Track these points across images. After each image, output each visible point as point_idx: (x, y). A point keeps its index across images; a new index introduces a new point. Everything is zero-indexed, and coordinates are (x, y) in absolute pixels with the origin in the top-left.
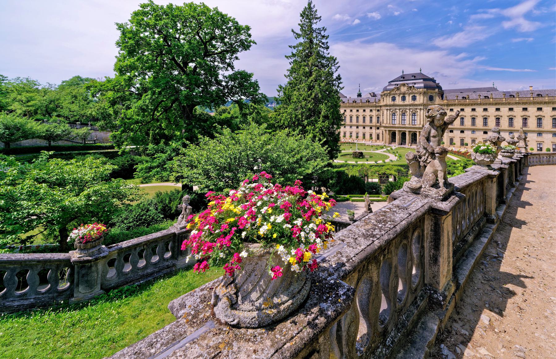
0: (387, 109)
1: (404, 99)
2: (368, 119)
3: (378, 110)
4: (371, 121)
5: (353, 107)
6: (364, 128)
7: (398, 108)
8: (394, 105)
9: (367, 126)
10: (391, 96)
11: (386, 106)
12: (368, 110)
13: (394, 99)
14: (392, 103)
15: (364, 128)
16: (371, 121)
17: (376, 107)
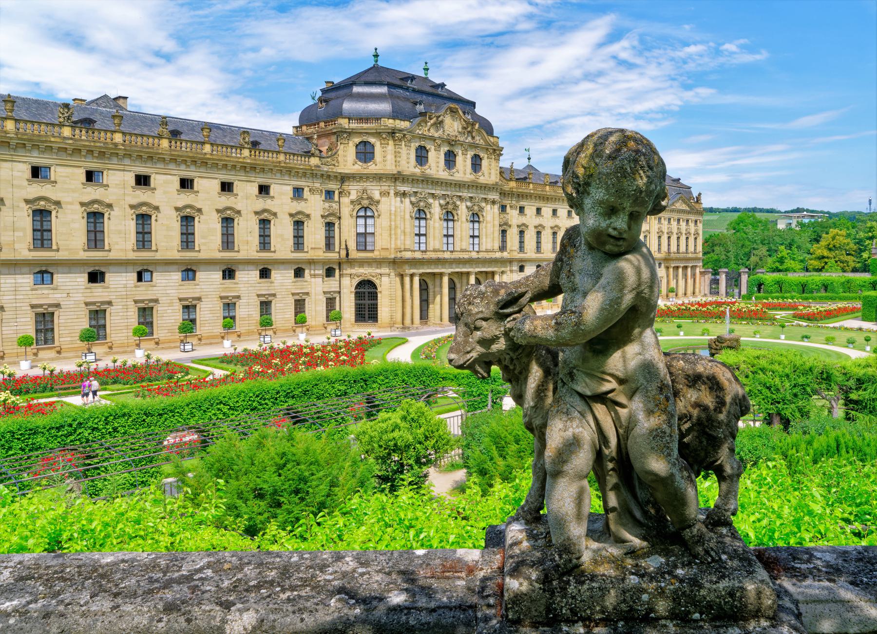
0: (404, 194)
1: (450, 159)
2: (282, 233)
3: (329, 194)
4: (299, 241)
5: (203, 163)
6: (265, 273)
7: (438, 192)
8: (427, 180)
9: (283, 263)
10: (415, 145)
11: (397, 178)
12: (282, 190)
13: (422, 156)
14: (418, 171)
15: (265, 273)
16: (299, 241)
17: (328, 177)
